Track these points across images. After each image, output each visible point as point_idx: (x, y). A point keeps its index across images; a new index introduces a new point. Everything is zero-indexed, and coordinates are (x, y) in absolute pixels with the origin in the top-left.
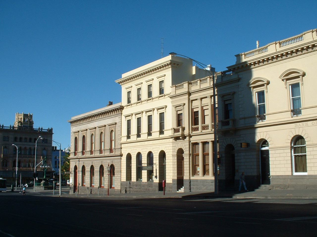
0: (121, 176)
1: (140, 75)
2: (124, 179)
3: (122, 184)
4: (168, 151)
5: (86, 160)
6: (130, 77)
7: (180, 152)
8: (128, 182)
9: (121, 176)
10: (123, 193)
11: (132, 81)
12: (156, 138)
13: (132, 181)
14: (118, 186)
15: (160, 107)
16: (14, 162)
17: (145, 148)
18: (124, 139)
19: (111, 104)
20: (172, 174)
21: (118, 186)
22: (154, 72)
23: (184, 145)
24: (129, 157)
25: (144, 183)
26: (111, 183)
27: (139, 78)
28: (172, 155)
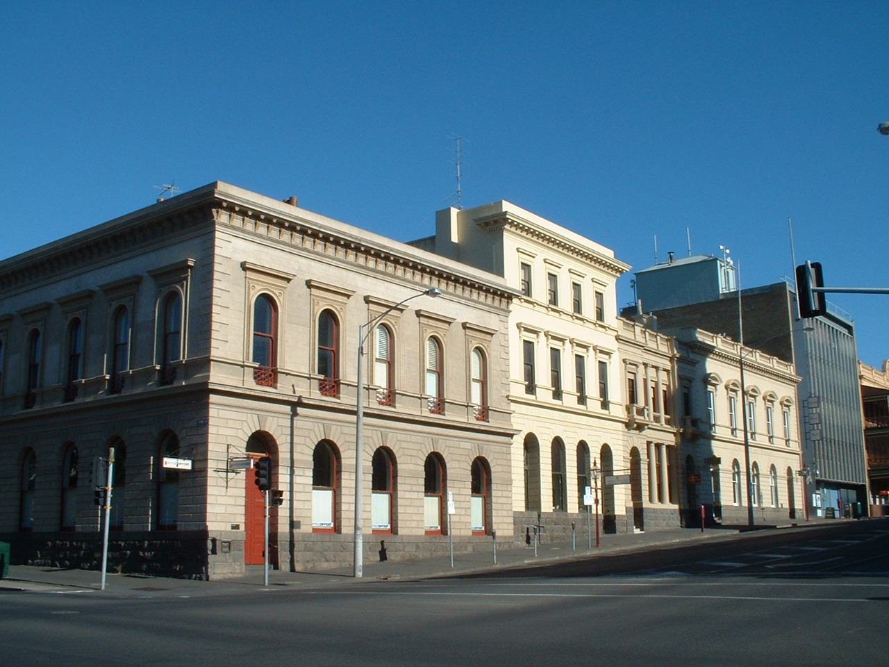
0: (511, 496)
1: (578, 253)
2: (519, 504)
3: (517, 518)
4: (617, 447)
5: (441, 435)
6: (526, 224)
7: (634, 452)
8: (535, 514)
9: (511, 496)
10: (520, 546)
11: (544, 246)
12: (545, 403)
13: (569, 511)
14: (505, 526)
15: (559, 334)
16: (634, 479)
17: (572, 429)
18: (519, 391)
19: (289, 202)
20: (623, 497)
21: (505, 526)
22: (525, 235)
23: (639, 440)
24: (531, 444)
25: (575, 515)
26: (393, 511)
27: (521, 236)
28: (624, 458)
